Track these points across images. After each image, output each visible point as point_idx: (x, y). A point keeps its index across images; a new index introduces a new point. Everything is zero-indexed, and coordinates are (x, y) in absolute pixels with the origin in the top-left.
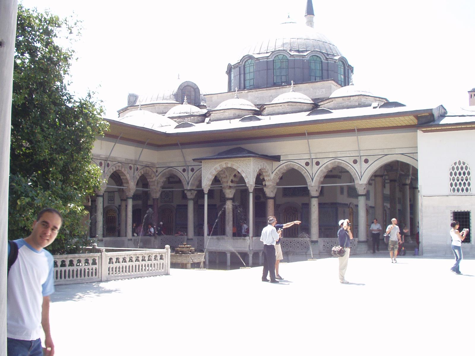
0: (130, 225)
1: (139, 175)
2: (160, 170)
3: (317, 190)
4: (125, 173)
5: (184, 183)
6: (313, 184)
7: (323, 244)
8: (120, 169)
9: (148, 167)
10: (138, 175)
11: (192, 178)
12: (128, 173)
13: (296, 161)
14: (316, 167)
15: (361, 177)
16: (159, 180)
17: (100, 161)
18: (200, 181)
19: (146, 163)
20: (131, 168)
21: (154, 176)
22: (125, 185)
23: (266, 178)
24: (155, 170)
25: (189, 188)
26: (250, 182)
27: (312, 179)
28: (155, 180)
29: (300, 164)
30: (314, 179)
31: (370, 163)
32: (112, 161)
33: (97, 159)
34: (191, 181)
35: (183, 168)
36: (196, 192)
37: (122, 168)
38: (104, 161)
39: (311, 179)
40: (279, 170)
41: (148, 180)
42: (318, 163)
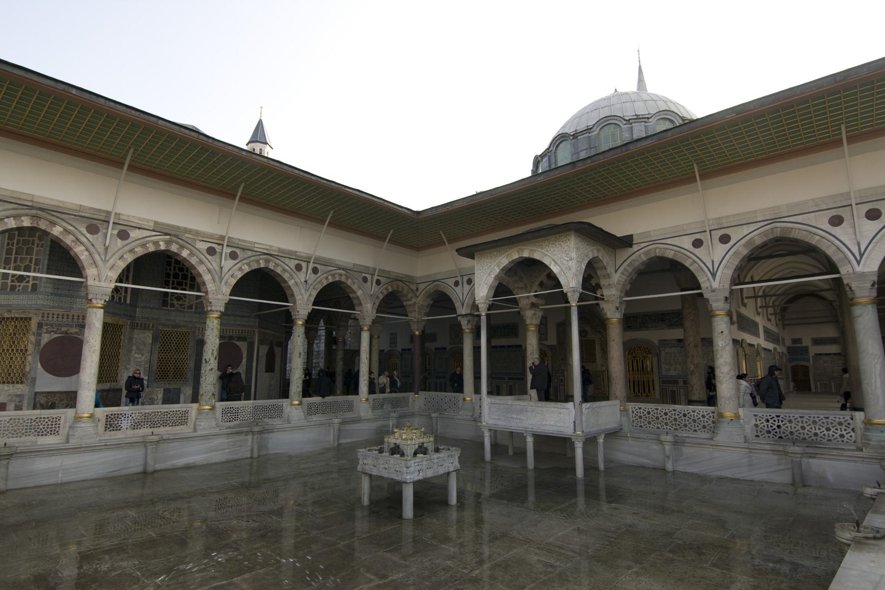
1: (382, 292)
3: (726, 298)
4: (355, 287)
5: (458, 305)
6: (715, 285)
7: (754, 422)
8: (343, 279)
10: (379, 292)
13: (669, 241)
14: (721, 249)
15: (861, 255)
17: (297, 262)
20: (365, 280)
21: (412, 297)
23: (603, 282)
25: (464, 313)
27: (714, 275)
28: (415, 303)
29: (680, 247)
30: (719, 274)
37: (347, 278)
39: (710, 275)
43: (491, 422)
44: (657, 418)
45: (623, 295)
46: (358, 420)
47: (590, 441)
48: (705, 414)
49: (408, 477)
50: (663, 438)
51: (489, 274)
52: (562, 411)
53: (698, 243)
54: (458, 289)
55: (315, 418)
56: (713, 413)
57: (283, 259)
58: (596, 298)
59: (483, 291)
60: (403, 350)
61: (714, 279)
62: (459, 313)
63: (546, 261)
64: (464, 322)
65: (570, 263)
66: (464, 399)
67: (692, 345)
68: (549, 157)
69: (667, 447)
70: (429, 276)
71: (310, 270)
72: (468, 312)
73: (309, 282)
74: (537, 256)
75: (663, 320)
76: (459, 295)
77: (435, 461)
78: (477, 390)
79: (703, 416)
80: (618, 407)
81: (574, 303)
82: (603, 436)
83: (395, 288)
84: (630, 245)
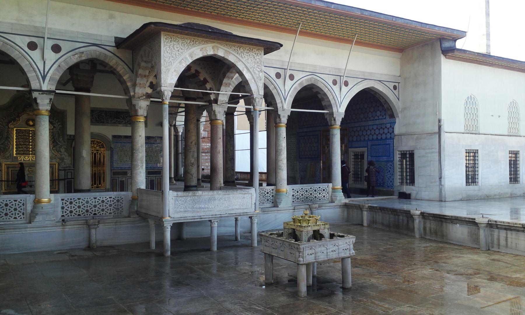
11: (55, 66)
14: (289, 83)
25: (45, 88)
27: (285, 99)
30: (287, 99)
31: (350, 86)
34: (51, 72)
35: (28, 40)
42: (292, 77)
51: (180, 62)
52: (245, 196)
54: (35, 54)
56: (273, 190)
72: (53, 88)
74: (232, 58)
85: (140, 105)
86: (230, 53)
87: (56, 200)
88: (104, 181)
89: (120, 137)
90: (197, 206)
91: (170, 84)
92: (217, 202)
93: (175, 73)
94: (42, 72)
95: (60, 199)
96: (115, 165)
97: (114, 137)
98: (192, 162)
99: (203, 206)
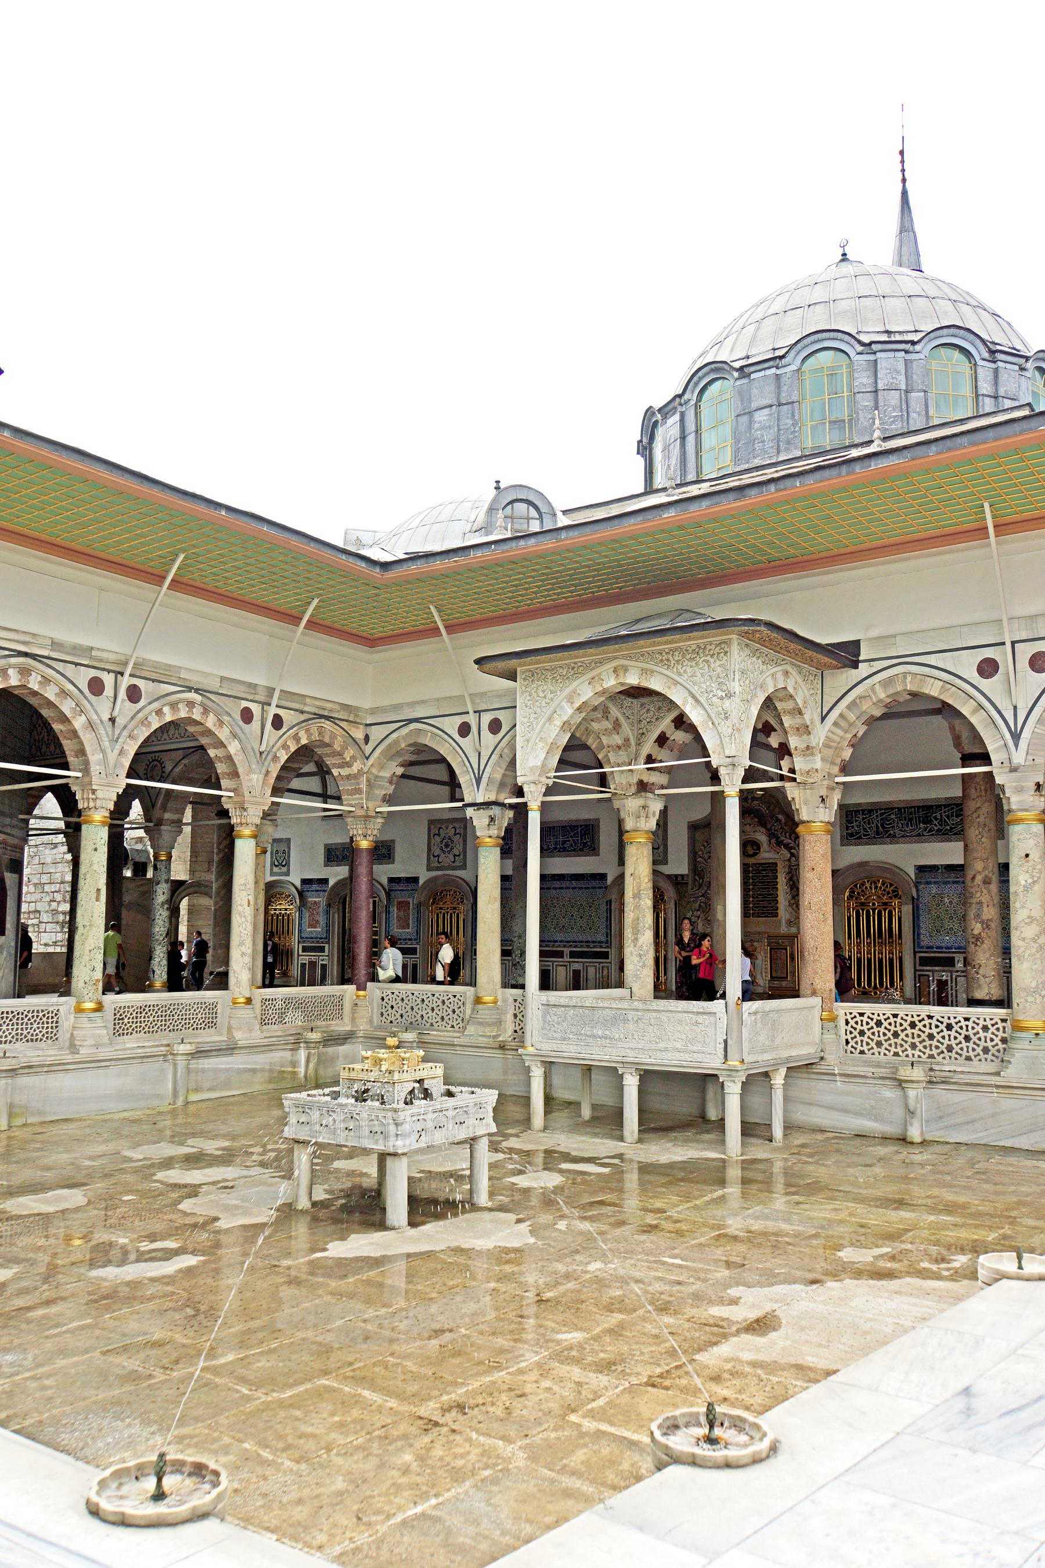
0: (242, 943)
2: (377, 733)
4: (223, 734)
6: (1019, 757)
8: (197, 715)
9: (327, 718)
12: (235, 736)
13: (931, 660)
16: (374, 771)
17: (93, 673)
18: (512, 763)
19: (317, 703)
20: (247, 716)
22: (224, 783)
24: (359, 734)
25: (480, 799)
26: (729, 747)
27: (1016, 737)
28: (360, 772)
30: (1026, 735)
32: (153, 681)
33: (77, 664)
34: (488, 769)
35: (458, 720)
36: (510, 814)
37: (206, 711)
38: (112, 675)
39: (1008, 736)
40: (850, 706)
41: (335, 772)
43: (547, 1047)
44: (896, 1035)
45: (836, 770)
46: (230, 1049)
47: (757, 1081)
48: (989, 1023)
49: (399, 1143)
50: (905, 1073)
51: (550, 719)
53: (988, 668)
55: (131, 1043)
56: (1004, 1021)
57: (60, 666)
58: (782, 778)
59: (536, 762)
60: (304, 881)
61: (1016, 746)
62: (468, 799)
63: (676, 696)
64: (479, 820)
65: (727, 703)
66: (478, 1000)
67: (979, 878)
68: (682, 415)
69: (911, 1093)
70: (397, 707)
71: (122, 694)
73: (120, 721)
75: (927, 821)
76: (471, 758)
77: (450, 1113)
78: (512, 979)
79: (985, 1028)
80: (817, 1012)
81: (732, 786)
82: (783, 1071)
83: (316, 737)
84: (855, 665)
85: (627, 808)
86: (652, 672)
87: (505, 1000)
88: (901, 979)
89: (933, 868)
90: (587, 1030)
91: (531, 769)
92: (631, 1026)
93: (541, 745)
94: (476, 771)
95: (511, 1000)
96: (925, 941)
97: (921, 869)
98: (976, 932)
99: (600, 1033)
